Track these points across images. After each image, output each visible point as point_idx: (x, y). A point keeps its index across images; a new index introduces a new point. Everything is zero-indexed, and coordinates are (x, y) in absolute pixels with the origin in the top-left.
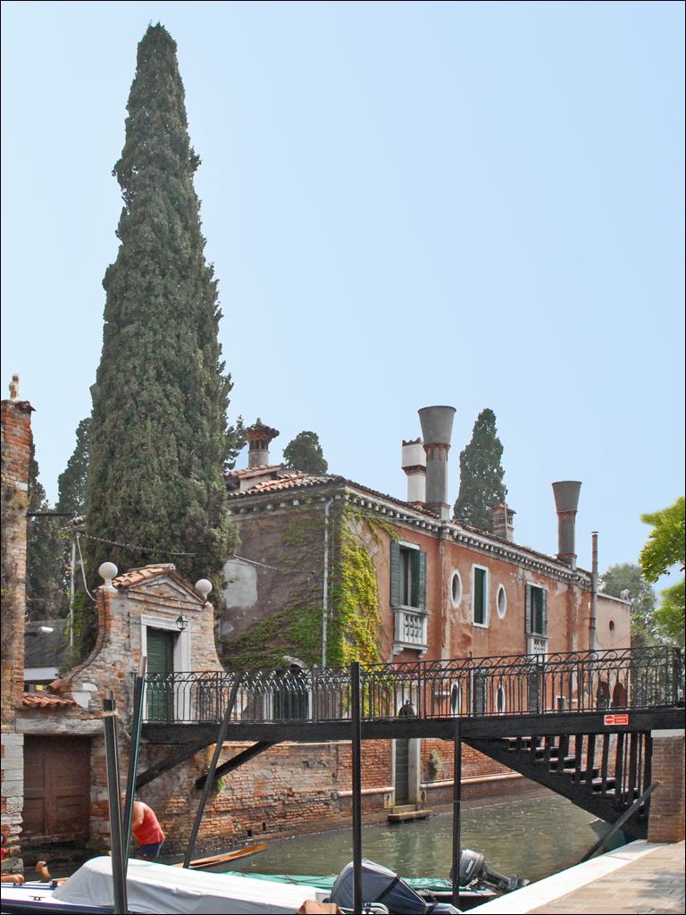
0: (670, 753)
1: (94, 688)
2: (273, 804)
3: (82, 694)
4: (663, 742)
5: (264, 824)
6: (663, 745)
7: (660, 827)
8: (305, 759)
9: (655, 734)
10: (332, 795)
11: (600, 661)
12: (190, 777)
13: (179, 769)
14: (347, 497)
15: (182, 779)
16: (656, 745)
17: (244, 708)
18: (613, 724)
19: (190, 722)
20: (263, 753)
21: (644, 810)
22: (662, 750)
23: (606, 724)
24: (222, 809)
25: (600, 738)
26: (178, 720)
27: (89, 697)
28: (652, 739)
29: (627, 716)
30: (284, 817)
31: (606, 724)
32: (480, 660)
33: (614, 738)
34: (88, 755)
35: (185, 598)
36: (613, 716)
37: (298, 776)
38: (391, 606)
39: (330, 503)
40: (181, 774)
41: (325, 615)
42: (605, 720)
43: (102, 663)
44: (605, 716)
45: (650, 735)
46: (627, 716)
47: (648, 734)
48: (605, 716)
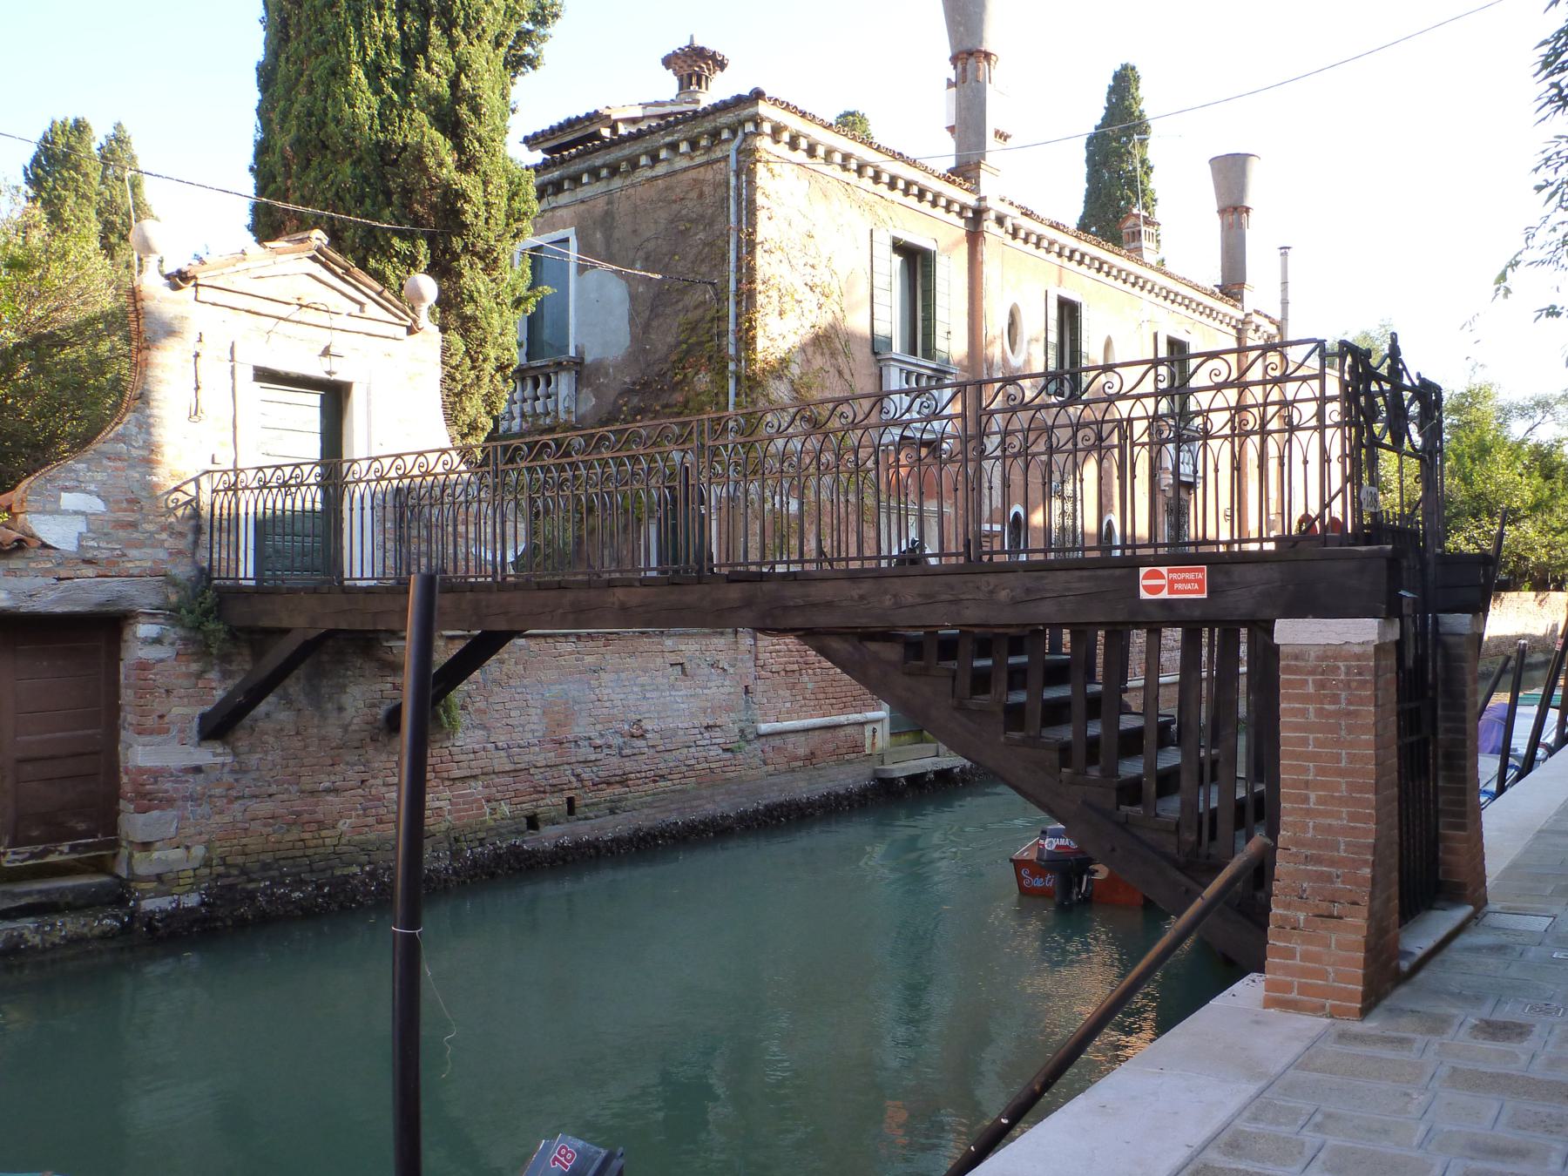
0: (1335, 699)
1: (97, 505)
2: (593, 757)
3: (59, 518)
4: (1312, 663)
5: (570, 801)
6: (1312, 672)
7: (1306, 957)
8: (673, 658)
9: (1288, 632)
10: (742, 731)
11: (1125, 397)
12: (373, 706)
13: (342, 689)
14: (767, 127)
15: (350, 711)
16: (1290, 670)
17: (521, 549)
18: (1164, 595)
19: (372, 583)
20: (494, 657)
21: (1260, 873)
22: (1311, 689)
23: (1144, 595)
24: (457, 773)
25: (1139, 638)
26: (351, 579)
27: (80, 526)
28: (1276, 649)
29: (1201, 572)
30: (623, 783)
31: (1144, 595)
32: (831, 406)
33: (1172, 637)
34: (115, 657)
35: (362, 310)
36: (1164, 570)
37: (655, 694)
38: (875, 353)
39: (737, 142)
40: (346, 700)
41: (732, 366)
42: (1143, 582)
43: (122, 447)
44: (1143, 571)
45: (1270, 632)
46: (1201, 572)
47: (1264, 628)
48: (1143, 571)
